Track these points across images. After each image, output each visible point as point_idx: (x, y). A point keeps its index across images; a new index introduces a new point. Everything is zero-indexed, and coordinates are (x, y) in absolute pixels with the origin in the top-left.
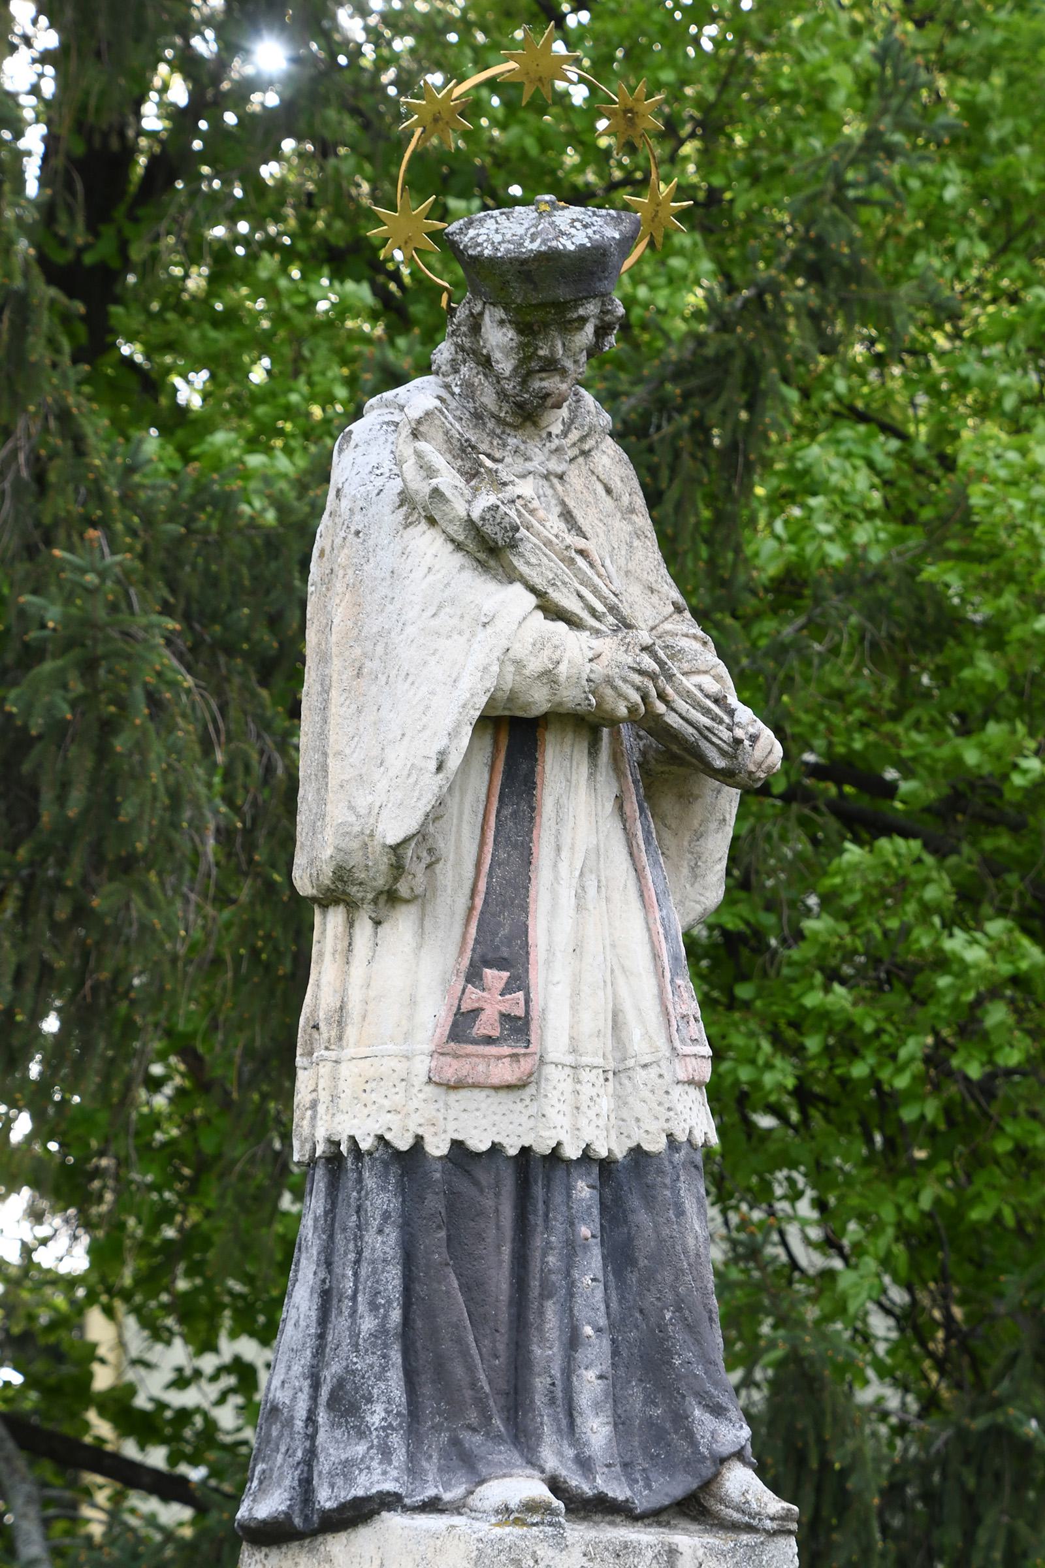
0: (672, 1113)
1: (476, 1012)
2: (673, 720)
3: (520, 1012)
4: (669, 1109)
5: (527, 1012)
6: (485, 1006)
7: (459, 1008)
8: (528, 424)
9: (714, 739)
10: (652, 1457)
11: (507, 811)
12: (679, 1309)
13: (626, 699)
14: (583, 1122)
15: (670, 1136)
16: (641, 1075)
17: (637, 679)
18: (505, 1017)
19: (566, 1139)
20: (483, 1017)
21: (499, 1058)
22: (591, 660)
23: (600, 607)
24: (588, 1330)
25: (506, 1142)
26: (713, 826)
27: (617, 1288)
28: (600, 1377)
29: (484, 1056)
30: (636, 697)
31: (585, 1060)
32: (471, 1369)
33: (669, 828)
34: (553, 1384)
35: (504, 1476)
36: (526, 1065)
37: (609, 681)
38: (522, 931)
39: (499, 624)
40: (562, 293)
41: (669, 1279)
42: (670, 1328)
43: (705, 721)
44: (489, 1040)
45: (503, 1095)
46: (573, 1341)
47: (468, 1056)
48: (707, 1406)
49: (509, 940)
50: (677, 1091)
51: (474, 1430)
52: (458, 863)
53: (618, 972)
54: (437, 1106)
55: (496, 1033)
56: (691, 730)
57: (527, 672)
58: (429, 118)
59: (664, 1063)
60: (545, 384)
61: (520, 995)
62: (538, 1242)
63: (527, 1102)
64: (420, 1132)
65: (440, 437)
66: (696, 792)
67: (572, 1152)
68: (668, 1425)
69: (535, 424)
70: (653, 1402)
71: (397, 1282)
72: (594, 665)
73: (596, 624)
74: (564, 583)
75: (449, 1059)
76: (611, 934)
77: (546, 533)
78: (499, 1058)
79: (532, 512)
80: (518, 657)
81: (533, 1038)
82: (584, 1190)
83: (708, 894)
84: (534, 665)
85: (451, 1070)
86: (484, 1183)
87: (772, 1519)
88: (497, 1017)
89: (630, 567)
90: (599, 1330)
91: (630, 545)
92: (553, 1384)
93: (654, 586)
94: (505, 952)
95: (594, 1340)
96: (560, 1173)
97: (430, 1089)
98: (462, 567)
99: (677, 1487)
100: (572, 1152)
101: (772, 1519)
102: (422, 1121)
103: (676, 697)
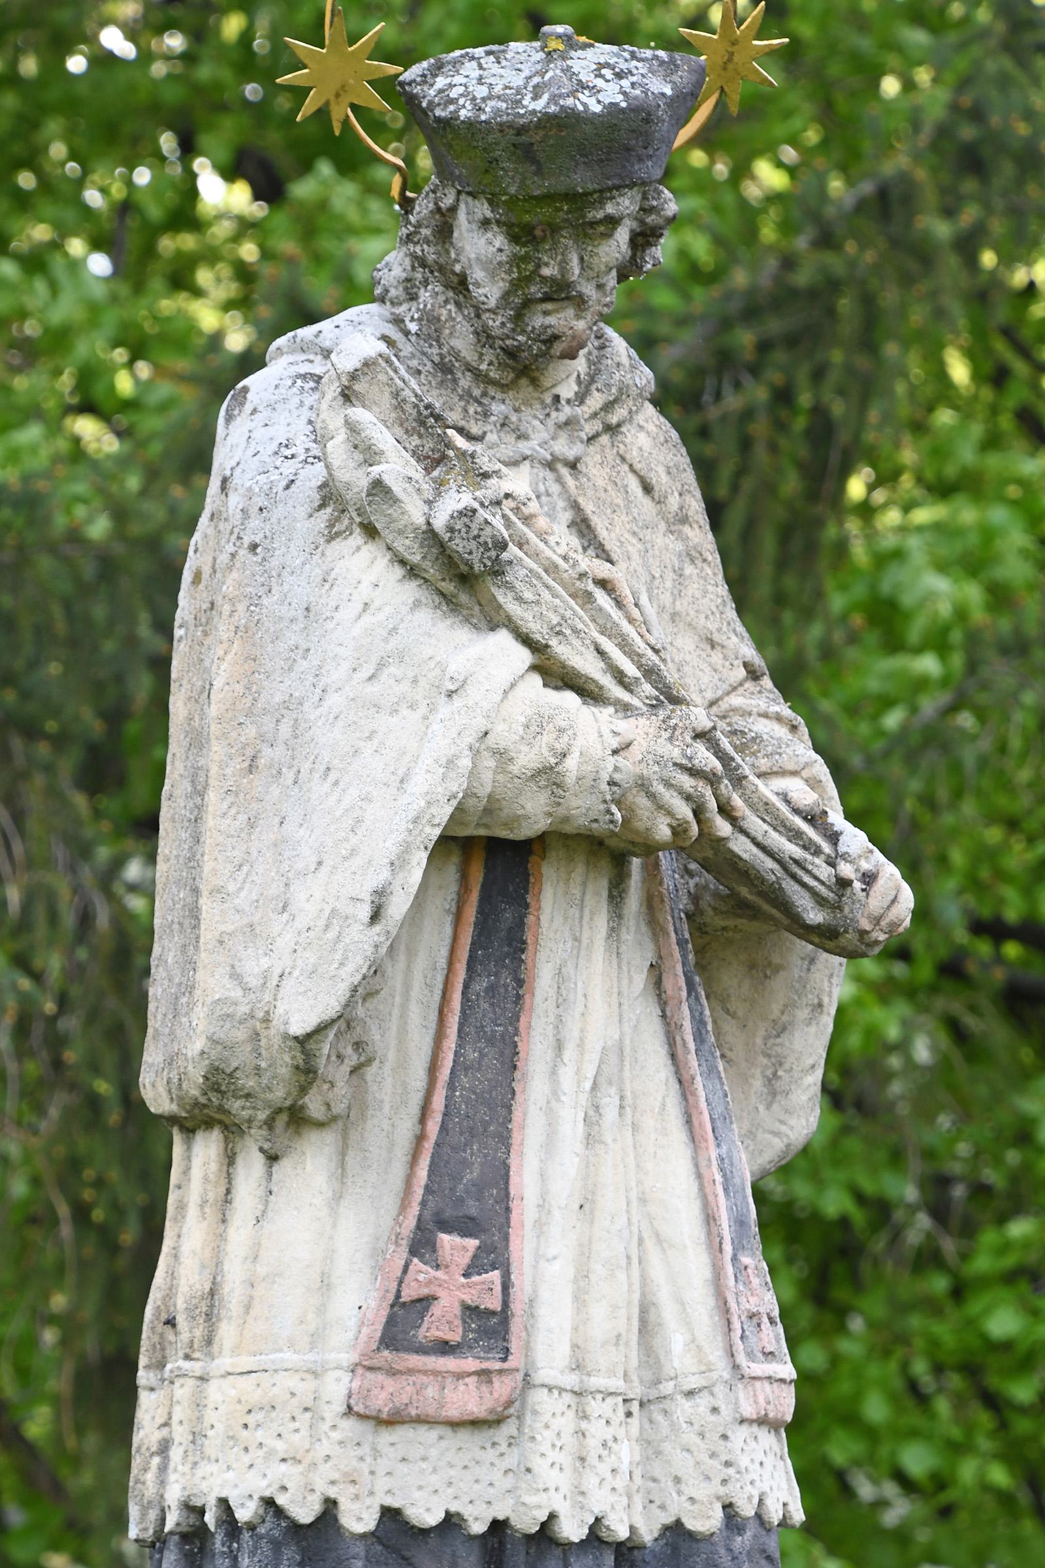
1: (425, 1302)
2: (742, 847)
3: (493, 1303)
4: (728, 1464)
5: (506, 1303)
6: (440, 1293)
7: (398, 1295)
8: (524, 382)
9: (807, 879)
11: (481, 985)
13: (670, 813)
15: (728, 1507)
17: (687, 782)
18: (471, 1311)
21: (460, 1376)
22: (615, 752)
23: (631, 670)
25: (468, 1512)
26: (803, 1014)
29: (435, 1373)
33: (733, 1016)
40: (581, 180)
43: (792, 849)
44: (445, 1348)
45: (464, 1435)
47: (410, 1372)
49: (479, 1189)
54: (359, 1452)
55: (455, 1337)
56: (770, 864)
57: (515, 769)
63: (503, 1448)
64: (332, 1493)
65: (386, 400)
66: (776, 959)
67: (572, 1530)
77: (548, 553)
78: (460, 1376)
79: (527, 520)
83: (793, 1122)
84: (527, 759)
94: (472, 1208)
97: (349, 1424)
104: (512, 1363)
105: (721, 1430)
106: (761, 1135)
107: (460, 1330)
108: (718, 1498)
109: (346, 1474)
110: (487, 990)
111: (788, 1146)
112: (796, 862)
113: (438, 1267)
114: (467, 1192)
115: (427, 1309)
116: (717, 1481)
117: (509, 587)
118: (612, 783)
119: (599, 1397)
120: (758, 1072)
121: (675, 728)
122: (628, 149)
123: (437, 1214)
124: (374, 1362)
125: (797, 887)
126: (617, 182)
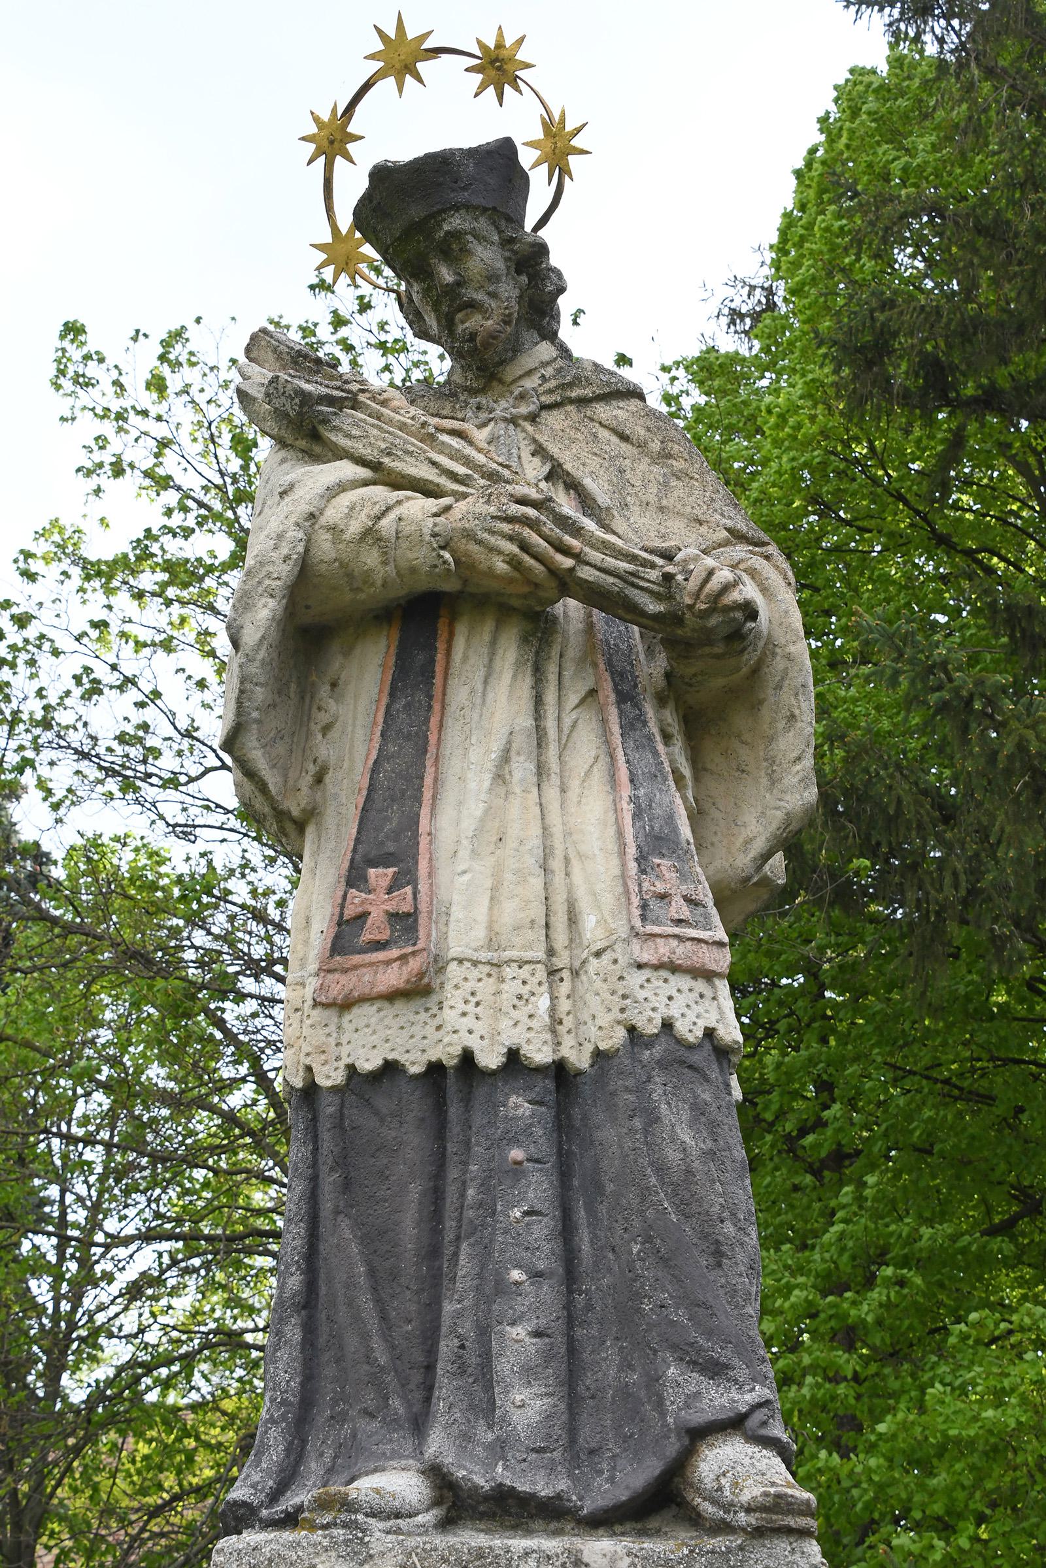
0: (628, 1001)
1: (363, 916)
2: (585, 573)
3: (406, 907)
4: (624, 997)
5: (416, 908)
6: (371, 909)
7: (342, 914)
8: (495, 383)
9: (642, 583)
10: (627, 1438)
11: (400, 704)
12: (648, 1239)
13: (500, 552)
14: (505, 1024)
15: (632, 1030)
16: (594, 963)
17: (506, 527)
18: (394, 917)
19: (473, 1042)
20: (369, 922)
21: (388, 963)
22: (436, 515)
23: (461, 470)
24: (516, 1275)
25: (403, 1058)
26: (781, 725)
27: (589, 1225)
28: (537, 1334)
29: (371, 964)
30: (515, 549)
31: (508, 954)
32: (365, 1337)
33: (746, 743)
34: (462, 1347)
35: (375, 1470)
36: (414, 964)
37: (469, 535)
38: (413, 821)
39: (298, 492)
40: (416, 212)
41: (635, 1203)
42: (638, 1264)
44: (379, 946)
45: (400, 1005)
47: (356, 967)
48: (695, 1363)
49: (396, 835)
50: (640, 977)
51: (372, 1416)
52: (351, 769)
53: (575, 862)
54: (327, 1030)
55: (384, 936)
56: (611, 580)
57: (347, 536)
58: (325, 143)
59: (619, 947)
60: (467, 325)
61: (408, 890)
62: (453, 1173)
63: (435, 1010)
64: (308, 1061)
65: (270, 356)
66: (762, 696)
67: (490, 1059)
68: (643, 1393)
69: (501, 382)
70: (630, 1366)
71: (298, 1242)
72: (441, 519)
73: (462, 489)
74: (406, 452)
75: (337, 975)
76: (564, 824)
77: (398, 417)
78: (388, 963)
79: (384, 403)
80: (331, 522)
81: (422, 933)
83: (788, 797)
84: (354, 528)
85: (339, 986)
86: (385, 1111)
87: (749, 1510)
88: (383, 918)
89: (664, 502)
90: (536, 1275)
91: (666, 484)
92: (462, 1347)
93: (701, 517)
94: (391, 847)
95: (527, 1287)
96: (481, 1092)
97: (317, 1013)
98: (284, 461)
100: (490, 1059)
101: (749, 1510)
102: (310, 1049)
103: (587, 549)
104: (421, 944)
105: (618, 974)
106: (768, 813)
107: (388, 932)
108: (619, 1023)
109: (317, 1047)
110: (404, 707)
111: (787, 814)
112: (632, 574)
113: (370, 892)
114: (387, 837)
115: (365, 923)
116: (616, 1010)
117: (337, 429)
118: (434, 535)
119: (515, 965)
120: (763, 774)
121: (490, 495)
122: (440, 185)
123: (364, 856)
124: (331, 966)
125: (637, 591)
126: (439, 207)
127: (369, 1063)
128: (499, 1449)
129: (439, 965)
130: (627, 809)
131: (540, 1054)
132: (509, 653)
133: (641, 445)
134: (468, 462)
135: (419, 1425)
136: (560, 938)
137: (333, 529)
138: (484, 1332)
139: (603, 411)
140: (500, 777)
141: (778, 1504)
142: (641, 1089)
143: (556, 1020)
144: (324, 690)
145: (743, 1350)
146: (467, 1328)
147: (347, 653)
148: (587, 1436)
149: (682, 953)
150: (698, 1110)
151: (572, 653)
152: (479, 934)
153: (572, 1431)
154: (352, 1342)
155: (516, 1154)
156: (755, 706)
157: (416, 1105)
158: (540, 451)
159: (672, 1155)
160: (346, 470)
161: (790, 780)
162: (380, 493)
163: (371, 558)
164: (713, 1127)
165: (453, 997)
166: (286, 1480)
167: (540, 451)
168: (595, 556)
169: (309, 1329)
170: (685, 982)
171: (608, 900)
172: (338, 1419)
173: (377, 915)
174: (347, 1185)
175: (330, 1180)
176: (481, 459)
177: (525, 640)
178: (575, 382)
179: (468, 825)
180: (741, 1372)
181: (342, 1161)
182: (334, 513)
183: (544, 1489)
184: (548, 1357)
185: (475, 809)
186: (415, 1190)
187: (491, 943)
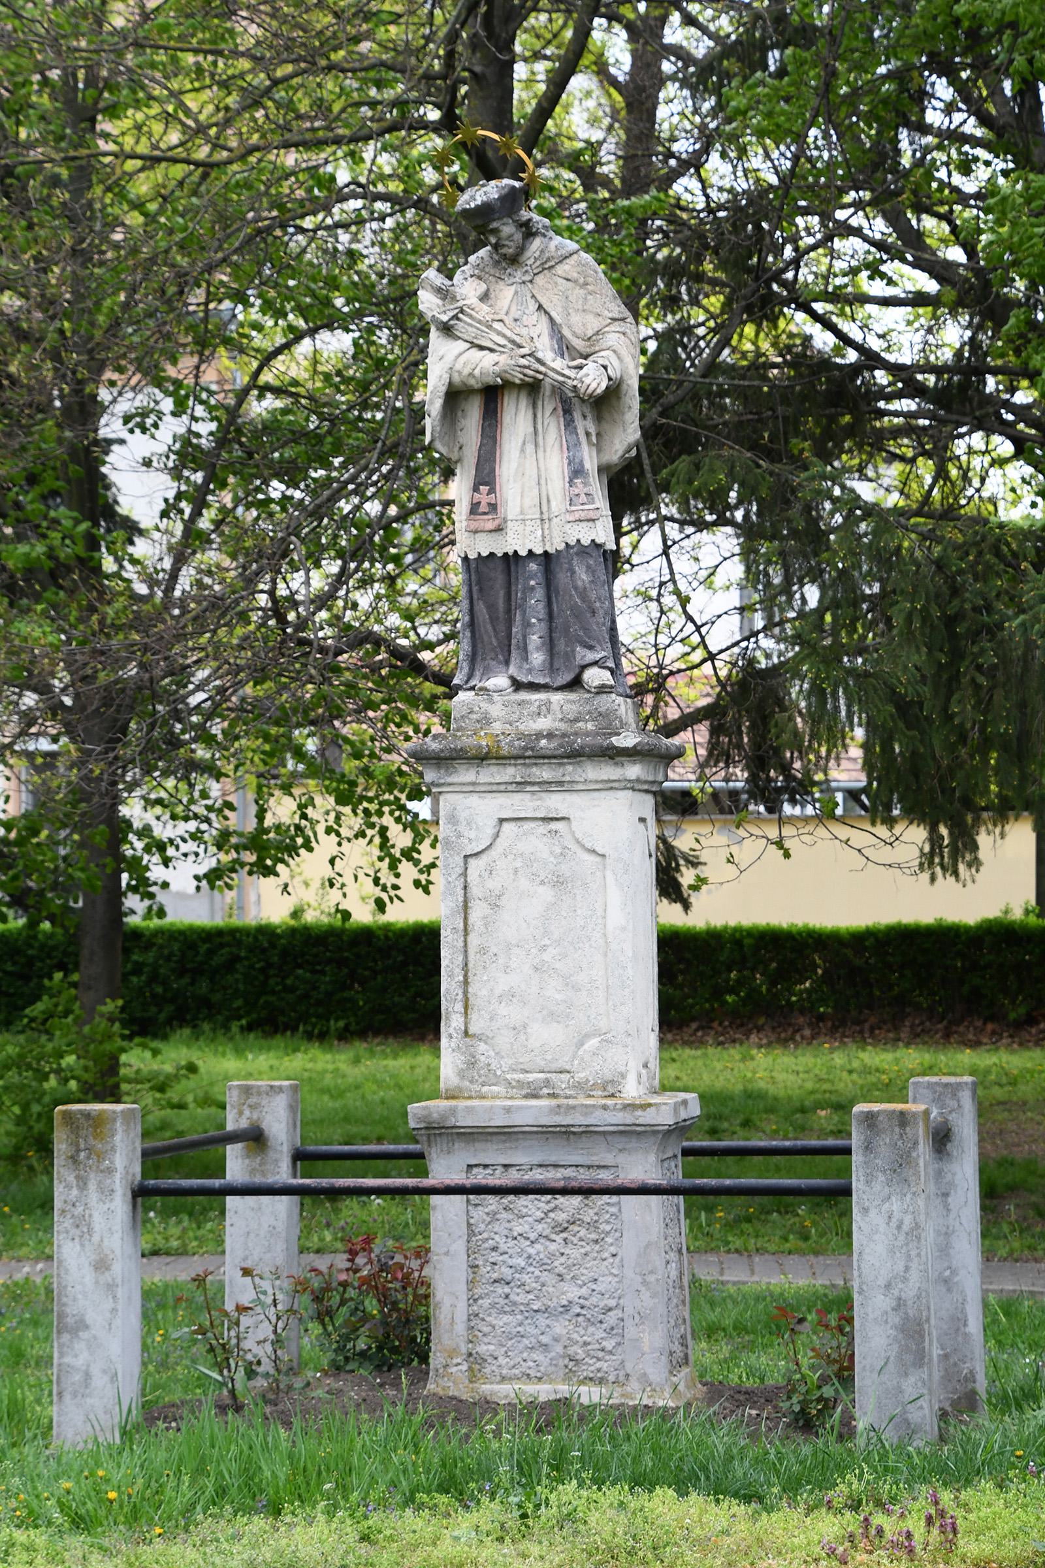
18: (489, 504)
23: (503, 341)
36: (497, 522)
43: (561, 379)
44: (485, 513)
46: (527, 625)
82: (533, 566)
84: (466, 372)
85: (474, 525)
99: (568, 677)
127: (484, 554)
128: (530, 671)
129: (505, 520)
130: (566, 462)
131: (539, 551)
132: (524, 402)
133: (576, 282)
134: (504, 336)
135: (507, 663)
136: (545, 509)
137: (459, 372)
138: (525, 637)
139: (560, 269)
140: (523, 451)
141: (603, 686)
142: (570, 563)
143: (543, 537)
144: (460, 414)
145: (599, 642)
146: (520, 636)
147: (466, 399)
148: (556, 665)
149: (583, 515)
150: (589, 567)
151: (548, 393)
152: (518, 510)
153: (551, 664)
154: (486, 639)
155: (532, 583)
156: (619, 398)
157: (500, 566)
158: (533, 296)
159: (580, 583)
160: (461, 346)
161: (630, 431)
162: (474, 350)
163: (472, 382)
164: (593, 572)
165: (510, 533)
166: (470, 677)
167: (533, 296)
168: (551, 374)
169: (473, 633)
170: (584, 524)
171: (559, 496)
172: (484, 659)
173: (483, 504)
174: (481, 590)
175: (475, 589)
176: (508, 333)
177: (529, 394)
178: (548, 260)
179: (512, 471)
180: (598, 648)
181: (479, 583)
182: (458, 367)
183: (542, 681)
184: (543, 644)
185: (514, 465)
186: (502, 593)
187: (522, 513)
